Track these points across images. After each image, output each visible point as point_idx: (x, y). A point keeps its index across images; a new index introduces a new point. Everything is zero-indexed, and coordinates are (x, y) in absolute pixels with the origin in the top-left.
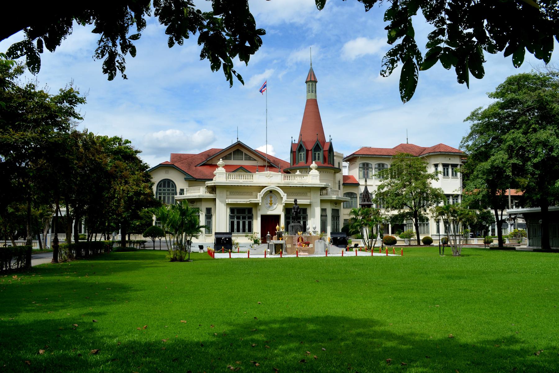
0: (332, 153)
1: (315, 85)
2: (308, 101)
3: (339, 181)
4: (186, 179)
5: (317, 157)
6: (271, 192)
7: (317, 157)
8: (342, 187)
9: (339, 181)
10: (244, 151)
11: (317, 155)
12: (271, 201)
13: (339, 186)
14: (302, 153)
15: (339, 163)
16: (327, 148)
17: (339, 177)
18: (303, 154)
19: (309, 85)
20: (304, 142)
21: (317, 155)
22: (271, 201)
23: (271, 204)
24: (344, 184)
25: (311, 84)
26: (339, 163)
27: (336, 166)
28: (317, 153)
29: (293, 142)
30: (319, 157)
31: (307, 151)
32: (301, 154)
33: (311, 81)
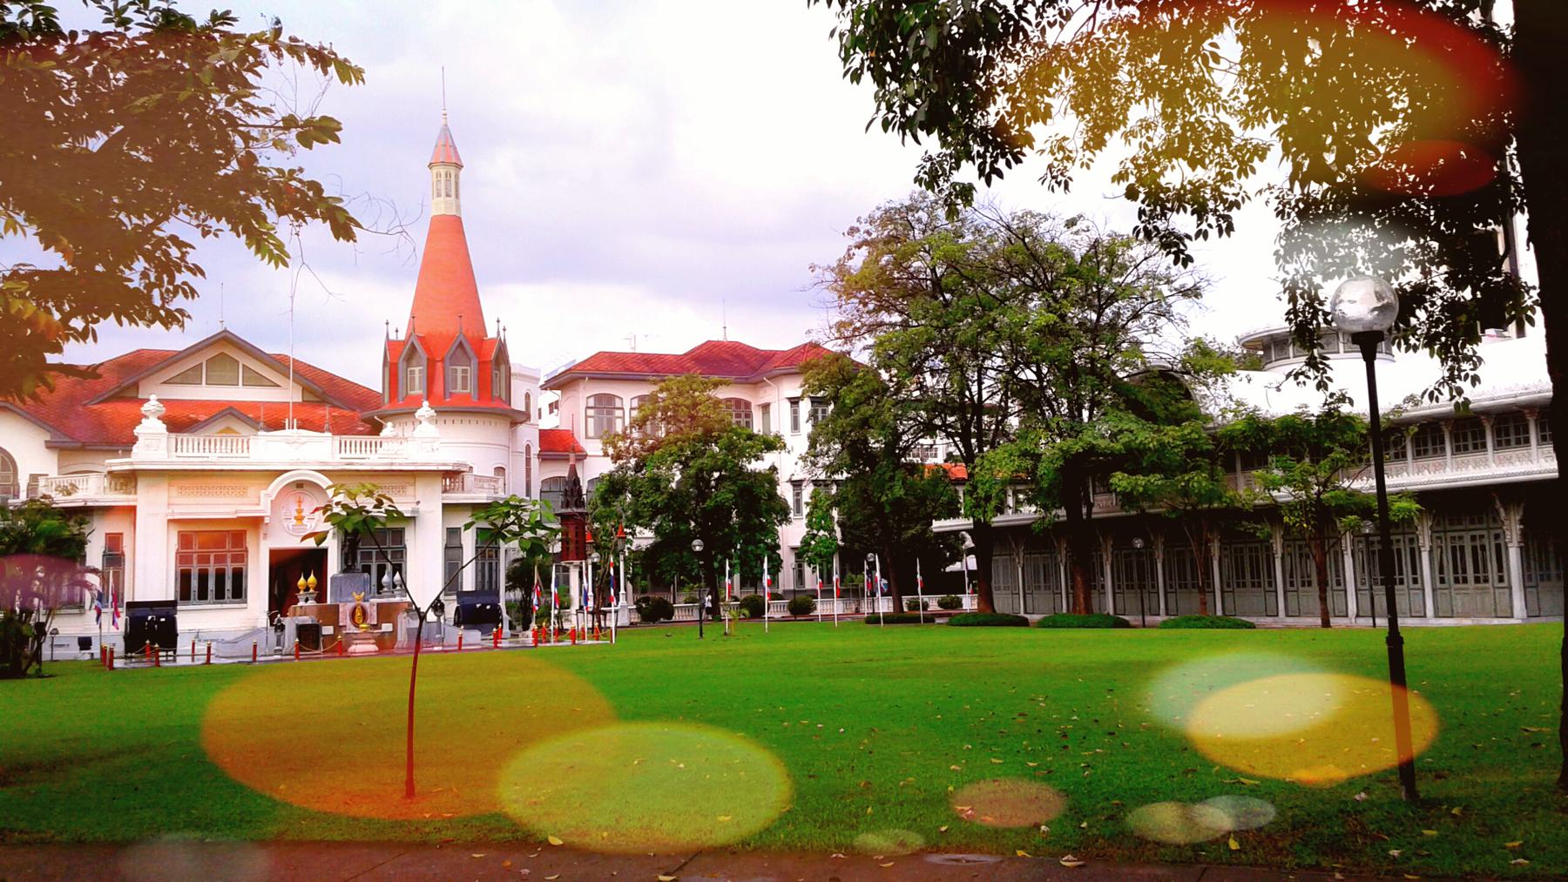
0: (503, 368)
1: (457, 177)
3: (528, 448)
4: (50, 446)
6: (300, 485)
8: (535, 462)
9: (528, 448)
10: (244, 360)
11: (460, 375)
12: (300, 511)
13: (528, 460)
14: (417, 369)
15: (528, 396)
18: (418, 372)
21: (460, 375)
22: (300, 511)
25: (442, 170)
26: (528, 396)
27: (518, 404)
28: (459, 369)
29: (393, 337)
32: (412, 372)
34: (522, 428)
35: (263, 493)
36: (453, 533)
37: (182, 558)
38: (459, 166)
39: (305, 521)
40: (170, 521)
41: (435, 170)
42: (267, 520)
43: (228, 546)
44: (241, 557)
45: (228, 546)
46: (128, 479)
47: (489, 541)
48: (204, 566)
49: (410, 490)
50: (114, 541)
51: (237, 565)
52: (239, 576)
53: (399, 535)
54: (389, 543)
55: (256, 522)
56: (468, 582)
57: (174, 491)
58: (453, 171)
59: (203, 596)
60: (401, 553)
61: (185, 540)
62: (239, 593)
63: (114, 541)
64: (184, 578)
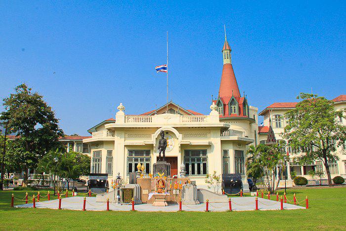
5: (233, 110)
7: (233, 110)
11: (233, 108)
13: (255, 135)
14: (221, 108)
16: (242, 101)
17: (255, 126)
20: (222, 99)
21: (233, 108)
24: (259, 133)
28: (233, 107)
30: (235, 110)
31: (225, 105)
34: (253, 124)
35: (153, 135)
36: (225, 152)
37: (129, 159)
40: (125, 146)
46: (112, 131)
47: (239, 155)
48: (136, 162)
49: (208, 135)
50: (110, 153)
51: (147, 162)
53: (205, 152)
54: (201, 155)
56: (232, 170)
57: (127, 135)
60: (205, 159)
61: (131, 152)
63: (110, 153)
64: (130, 165)
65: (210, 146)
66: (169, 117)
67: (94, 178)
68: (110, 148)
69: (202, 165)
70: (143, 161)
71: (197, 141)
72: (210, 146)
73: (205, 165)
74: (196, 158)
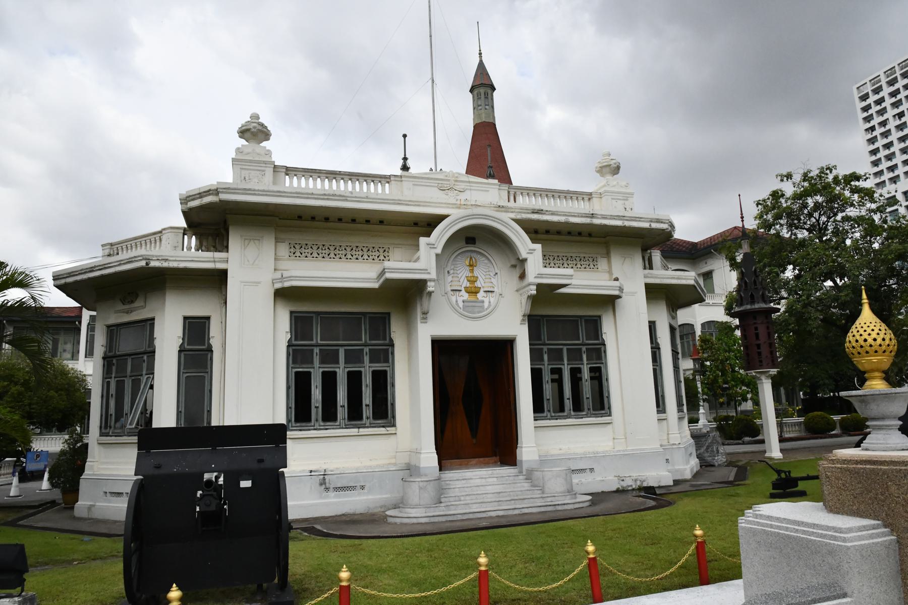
1: (492, 96)
2: (476, 127)
19: (479, 94)
22: (473, 280)
23: (473, 291)
25: (482, 90)
33: (482, 85)
35: (423, 240)
36: (652, 326)
38: (494, 89)
39: (481, 295)
41: (475, 92)
42: (431, 287)
43: (365, 337)
44: (385, 354)
45: (365, 337)
48: (329, 368)
49: (603, 264)
51: (379, 367)
52: (382, 384)
53: (594, 326)
55: (407, 295)
57: (284, 250)
58: (489, 91)
59: (329, 415)
60: (598, 352)
62: (383, 412)
63: (196, 330)
65: (609, 302)
66: (461, 186)
67: (176, 462)
68: (196, 306)
69: (586, 374)
70: (361, 361)
71: (581, 280)
72: (609, 302)
73: (598, 376)
74: (564, 345)
